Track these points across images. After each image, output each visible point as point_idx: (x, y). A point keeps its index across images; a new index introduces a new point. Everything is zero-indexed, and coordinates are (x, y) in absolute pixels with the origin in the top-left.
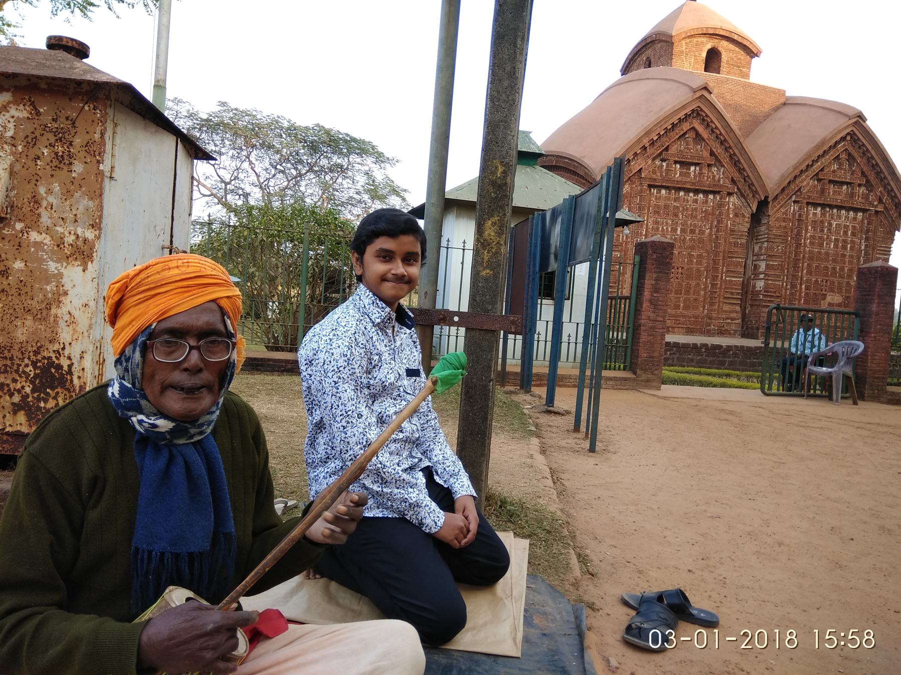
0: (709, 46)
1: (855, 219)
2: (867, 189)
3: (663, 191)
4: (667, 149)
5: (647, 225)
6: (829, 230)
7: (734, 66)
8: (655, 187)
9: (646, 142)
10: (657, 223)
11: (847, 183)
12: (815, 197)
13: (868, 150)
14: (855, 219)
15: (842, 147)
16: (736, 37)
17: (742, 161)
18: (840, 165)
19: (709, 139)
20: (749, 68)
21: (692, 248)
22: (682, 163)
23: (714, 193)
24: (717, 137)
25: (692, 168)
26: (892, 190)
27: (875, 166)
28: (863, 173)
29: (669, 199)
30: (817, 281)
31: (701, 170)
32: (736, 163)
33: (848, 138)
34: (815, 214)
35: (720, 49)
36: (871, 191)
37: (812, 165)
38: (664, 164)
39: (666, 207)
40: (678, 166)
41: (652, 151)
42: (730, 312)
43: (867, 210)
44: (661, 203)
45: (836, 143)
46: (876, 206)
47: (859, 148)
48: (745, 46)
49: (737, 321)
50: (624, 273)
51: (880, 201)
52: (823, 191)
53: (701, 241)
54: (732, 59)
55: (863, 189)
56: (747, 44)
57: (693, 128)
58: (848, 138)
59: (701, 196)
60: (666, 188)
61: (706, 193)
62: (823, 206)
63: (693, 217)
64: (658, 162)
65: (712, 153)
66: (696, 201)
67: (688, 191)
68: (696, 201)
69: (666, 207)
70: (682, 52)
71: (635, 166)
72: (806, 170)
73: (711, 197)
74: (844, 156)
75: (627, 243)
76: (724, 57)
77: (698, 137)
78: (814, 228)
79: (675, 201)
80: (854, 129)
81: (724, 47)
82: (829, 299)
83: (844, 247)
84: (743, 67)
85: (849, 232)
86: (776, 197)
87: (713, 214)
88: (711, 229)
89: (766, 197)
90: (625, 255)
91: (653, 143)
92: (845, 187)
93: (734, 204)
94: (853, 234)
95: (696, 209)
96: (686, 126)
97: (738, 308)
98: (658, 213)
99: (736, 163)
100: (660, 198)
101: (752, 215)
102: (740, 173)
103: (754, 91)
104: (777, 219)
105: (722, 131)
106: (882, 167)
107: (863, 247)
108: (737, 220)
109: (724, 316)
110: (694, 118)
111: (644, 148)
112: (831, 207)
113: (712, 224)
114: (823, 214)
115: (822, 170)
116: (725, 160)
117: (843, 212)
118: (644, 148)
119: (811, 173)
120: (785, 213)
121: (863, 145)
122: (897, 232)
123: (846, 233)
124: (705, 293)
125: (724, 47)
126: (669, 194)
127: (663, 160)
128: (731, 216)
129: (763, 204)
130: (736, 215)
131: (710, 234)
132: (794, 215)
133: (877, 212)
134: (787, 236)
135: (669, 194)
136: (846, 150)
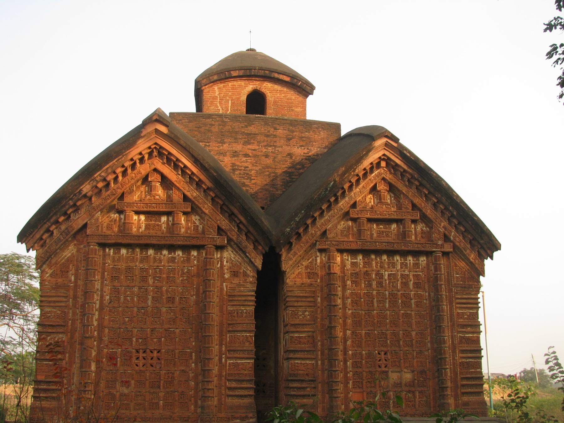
1: (416, 265)
2: (427, 226)
3: (124, 251)
5: (102, 297)
6: (380, 284)
8: (110, 246)
11: (397, 221)
12: (352, 242)
14: (416, 265)
15: (377, 176)
24: (190, 178)
28: (414, 206)
29: (133, 260)
30: (369, 355)
33: (383, 164)
34: (353, 264)
35: (263, 90)
36: (431, 228)
38: (122, 216)
39: (129, 269)
43: (431, 253)
47: (402, 175)
52: (359, 231)
55: (420, 227)
57: (155, 170)
58: (383, 164)
59: (179, 253)
60: (127, 246)
61: (186, 248)
62: (366, 253)
66: (172, 260)
67: (158, 248)
68: (172, 260)
69: (129, 269)
73: (194, 253)
74: (382, 187)
76: (270, 98)
80: (387, 153)
81: (267, 88)
83: (406, 304)
88: (197, 295)
90: (72, 337)
92: (394, 226)
93: (229, 260)
100: (119, 260)
101: (258, 272)
108: (236, 281)
112: (378, 253)
114: (367, 264)
115: (354, 205)
117: (397, 258)
122: (481, 277)
123: (405, 284)
124: (197, 384)
125: (267, 88)
126: (133, 252)
128: (226, 276)
130: (235, 274)
133: (446, 254)
135: (133, 252)
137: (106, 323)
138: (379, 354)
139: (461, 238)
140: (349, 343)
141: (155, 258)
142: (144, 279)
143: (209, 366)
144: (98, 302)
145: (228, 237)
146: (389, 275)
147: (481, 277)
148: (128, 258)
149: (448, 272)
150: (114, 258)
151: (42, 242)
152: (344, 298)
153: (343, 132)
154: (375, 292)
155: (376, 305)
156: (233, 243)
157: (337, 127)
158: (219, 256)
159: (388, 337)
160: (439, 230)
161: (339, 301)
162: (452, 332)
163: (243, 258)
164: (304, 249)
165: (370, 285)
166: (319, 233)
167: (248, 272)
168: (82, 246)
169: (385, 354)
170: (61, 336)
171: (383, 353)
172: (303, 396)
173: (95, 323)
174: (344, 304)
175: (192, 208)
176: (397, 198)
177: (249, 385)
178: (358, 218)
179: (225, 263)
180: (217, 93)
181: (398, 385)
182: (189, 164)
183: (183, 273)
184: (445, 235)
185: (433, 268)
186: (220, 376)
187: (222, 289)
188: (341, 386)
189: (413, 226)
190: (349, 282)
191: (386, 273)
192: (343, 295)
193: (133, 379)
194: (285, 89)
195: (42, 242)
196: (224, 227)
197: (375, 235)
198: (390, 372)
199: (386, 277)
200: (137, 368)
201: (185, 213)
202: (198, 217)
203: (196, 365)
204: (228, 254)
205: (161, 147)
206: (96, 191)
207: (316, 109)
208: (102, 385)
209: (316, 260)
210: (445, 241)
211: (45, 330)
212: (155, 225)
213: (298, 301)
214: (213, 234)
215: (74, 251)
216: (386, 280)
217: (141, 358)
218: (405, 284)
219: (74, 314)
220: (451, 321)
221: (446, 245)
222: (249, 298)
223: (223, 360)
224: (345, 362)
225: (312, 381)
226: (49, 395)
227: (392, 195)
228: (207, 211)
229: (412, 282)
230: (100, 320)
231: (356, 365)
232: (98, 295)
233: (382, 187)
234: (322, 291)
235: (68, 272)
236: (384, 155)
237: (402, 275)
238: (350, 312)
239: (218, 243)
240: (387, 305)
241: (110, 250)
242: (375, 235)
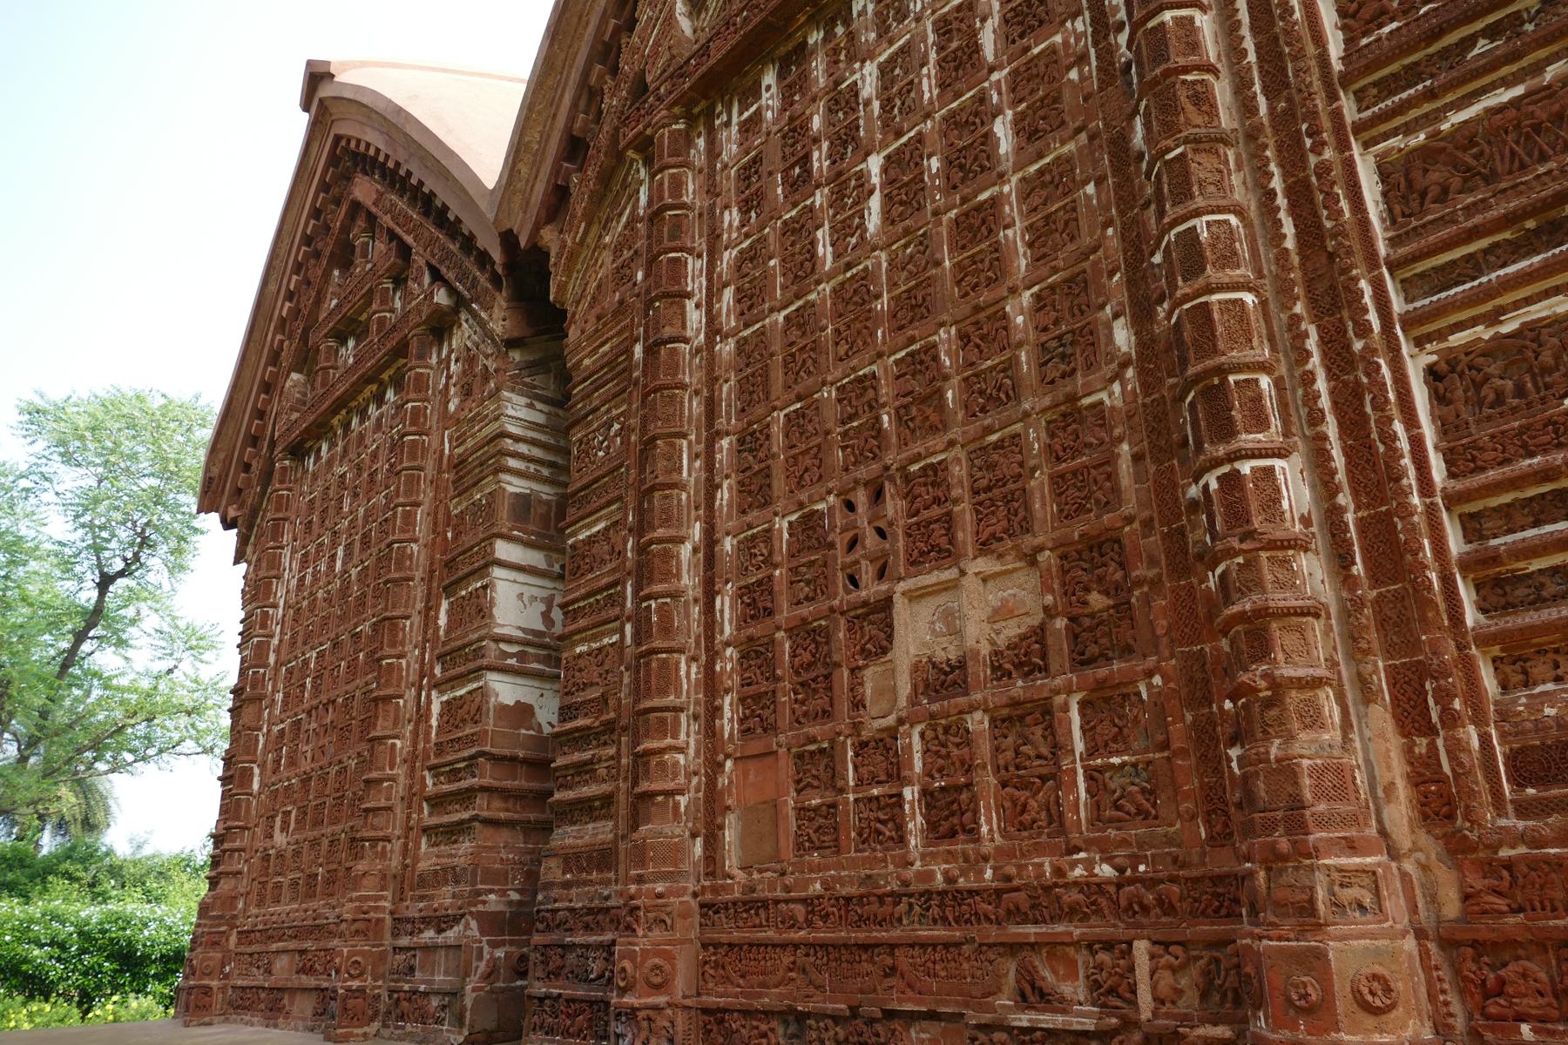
30: (809, 524)
82: (916, 634)
129: (525, 273)
161: (695, 317)
162: (1293, 159)
169: (877, 496)
171: (861, 497)
174: (712, 318)
181: (944, 679)
186: (411, 760)
188: (688, 733)
190: (732, 217)
198: (899, 603)
216: (868, 103)
220: (1276, 84)
224: (710, 593)
231: (756, 603)
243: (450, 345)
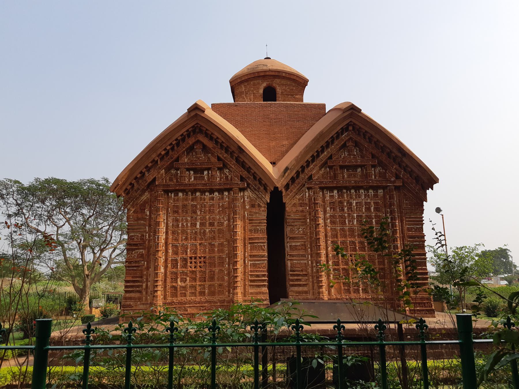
0: (265, 84)
1: (376, 196)
3: (180, 194)
4: (177, 160)
7: (288, 95)
8: (171, 192)
9: (154, 156)
10: (177, 221)
11: (361, 166)
13: (372, 136)
14: (376, 196)
16: (284, 75)
17: (246, 161)
18: (350, 152)
19: (214, 148)
20: (302, 95)
21: (214, 238)
22: (196, 171)
23: (229, 190)
24: (221, 145)
25: (206, 173)
26: (407, 166)
27: (383, 149)
29: (186, 200)
31: (212, 173)
32: (243, 165)
33: (351, 128)
34: (332, 197)
35: (274, 85)
36: (386, 170)
37: (318, 156)
38: (179, 172)
39: (184, 206)
40: (192, 172)
41: (167, 162)
42: (257, 293)
44: (180, 204)
45: (338, 135)
46: (394, 182)
48: (294, 80)
49: (265, 302)
50: (148, 268)
51: (397, 177)
53: (220, 231)
54: (286, 91)
56: (295, 78)
57: (198, 142)
58: (351, 128)
59: (216, 194)
60: (183, 191)
62: (340, 189)
63: (211, 212)
64: (173, 172)
65: (219, 159)
70: (242, 93)
71: (149, 177)
72: (313, 161)
73: (226, 193)
75: (149, 241)
76: (279, 90)
77: (205, 148)
78: (333, 208)
79: (192, 200)
80: (354, 121)
84: (296, 95)
85: (372, 209)
86: (287, 187)
87: (229, 207)
88: (229, 221)
89: (276, 188)
90: (149, 251)
91: (162, 158)
92: (359, 170)
94: (376, 209)
95: (213, 205)
96: (191, 141)
97: (265, 290)
98: (177, 212)
99: (243, 165)
100: (178, 200)
102: (249, 172)
103: (296, 109)
104: (294, 205)
105: (223, 139)
106: (390, 147)
107: (389, 220)
108: (254, 210)
109: (250, 298)
110: (198, 132)
111: (155, 162)
112: (348, 189)
113: (229, 216)
114: (341, 195)
115: (330, 157)
116: (232, 164)
117: (362, 191)
118: (155, 162)
119: (318, 162)
120: (302, 199)
121: (366, 132)
122: (424, 202)
123: (368, 209)
124: (229, 278)
126: (187, 195)
127: (177, 169)
128: (247, 207)
130: (253, 206)
131: (229, 225)
132: (310, 200)
133: (397, 188)
134: (305, 219)
136: (351, 138)
137: (170, 241)
138: (351, 256)
139: (409, 175)
140: (329, 249)
141: (201, 198)
142: (195, 212)
143: (236, 266)
144: (165, 228)
145: (247, 182)
146: (356, 203)
147: (424, 202)
148: (183, 198)
149: (399, 200)
150: (174, 199)
151: (127, 191)
152: (325, 219)
153: (327, 110)
154: (346, 215)
155: (347, 222)
156: (250, 186)
157: (323, 106)
158: (242, 194)
159: (357, 245)
160: (392, 171)
163: (257, 195)
164: (297, 188)
165: (343, 210)
166: (307, 177)
167: (261, 204)
168: (153, 192)
170: (141, 251)
172: (300, 285)
173: (163, 241)
175: (224, 165)
176: (361, 150)
177: (263, 278)
178: (334, 166)
179: (246, 199)
180: (244, 89)
182: (219, 136)
183: (219, 207)
184: (396, 174)
185: (388, 197)
187: (244, 216)
189: (373, 169)
190: (328, 209)
191: (354, 202)
192: (325, 218)
193: (188, 276)
194: (289, 83)
195: (127, 191)
196: (244, 176)
197: (346, 176)
199: (354, 204)
200: (191, 269)
201: (220, 169)
202: (227, 170)
203: (229, 265)
204: (248, 193)
205: (201, 126)
206: (160, 157)
207: (310, 96)
208: (169, 280)
209: (306, 195)
210: (396, 178)
211: (131, 247)
212: (200, 177)
213: (294, 222)
214: (237, 180)
215: (149, 196)
217: (193, 262)
218: (368, 209)
219: (149, 236)
221: (397, 181)
222: (262, 221)
223: (246, 262)
225: (306, 275)
226: (134, 289)
227: (358, 149)
228: (233, 166)
229: (373, 207)
230: (166, 239)
232: (164, 223)
233: (350, 144)
234: (310, 214)
235: (145, 209)
236: (351, 121)
237: (365, 202)
238: (330, 228)
239: (241, 186)
240: (355, 223)
241: (171, 194)
242: (346, 176)
243: (244, 193)
